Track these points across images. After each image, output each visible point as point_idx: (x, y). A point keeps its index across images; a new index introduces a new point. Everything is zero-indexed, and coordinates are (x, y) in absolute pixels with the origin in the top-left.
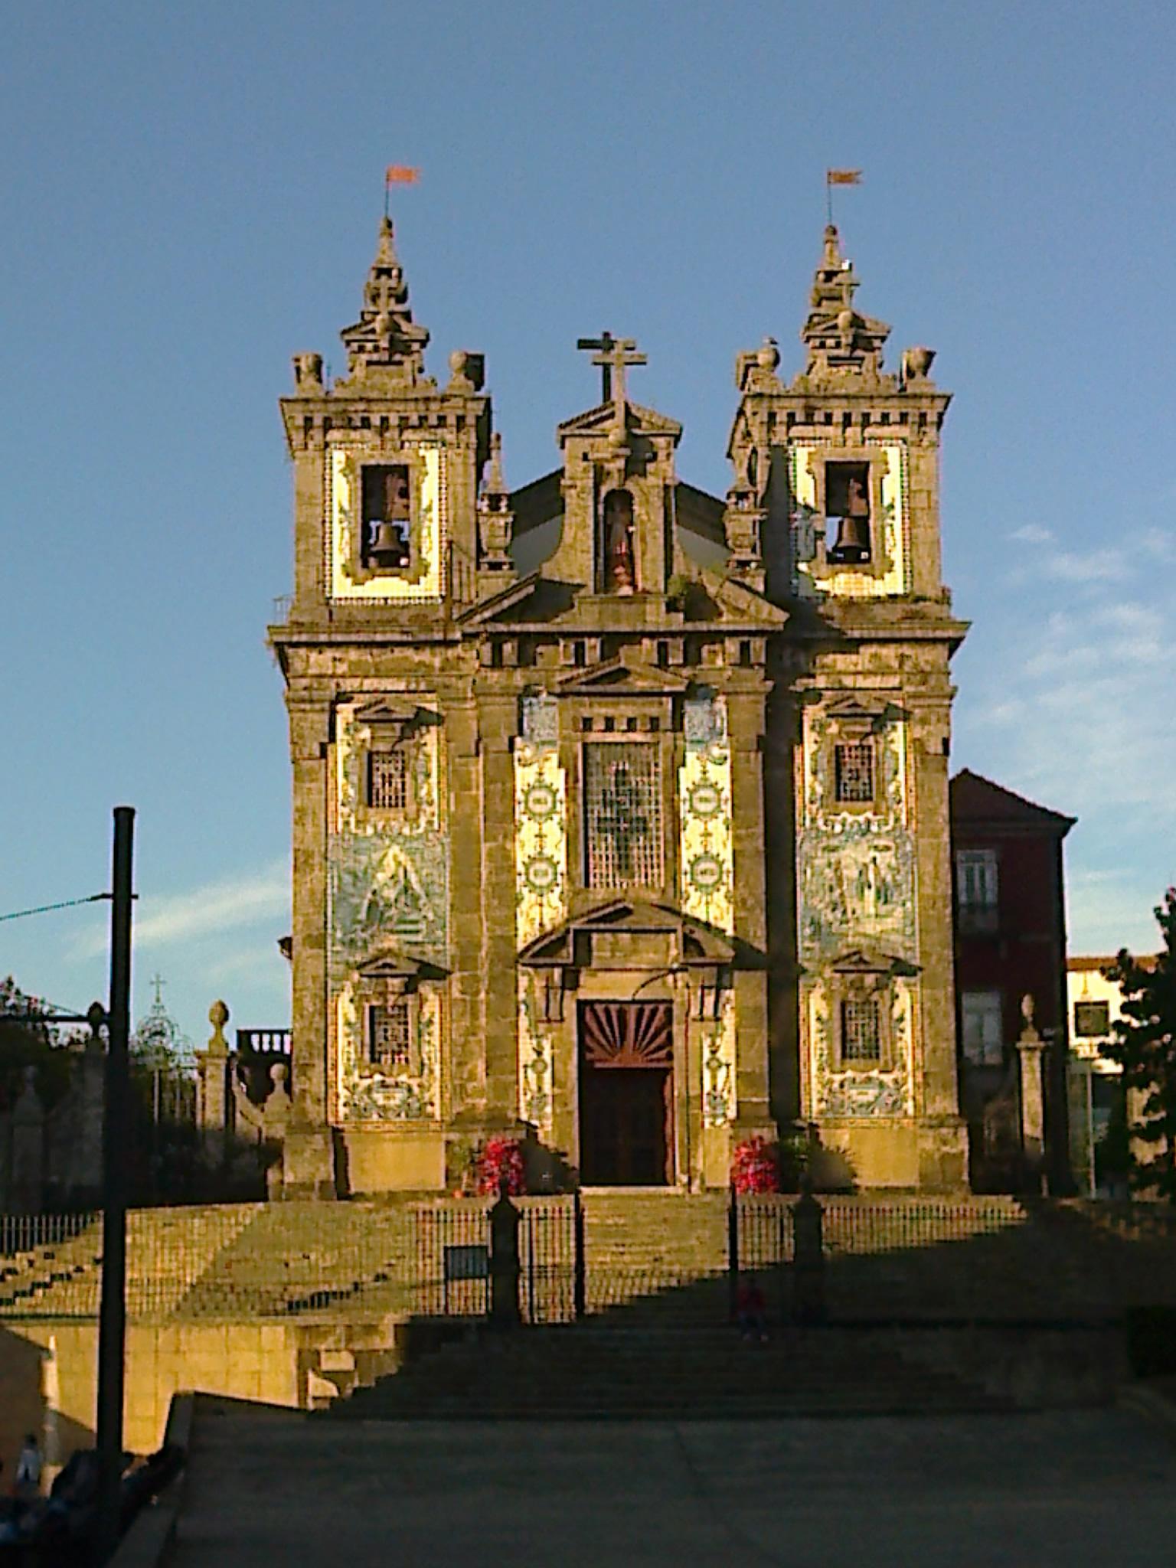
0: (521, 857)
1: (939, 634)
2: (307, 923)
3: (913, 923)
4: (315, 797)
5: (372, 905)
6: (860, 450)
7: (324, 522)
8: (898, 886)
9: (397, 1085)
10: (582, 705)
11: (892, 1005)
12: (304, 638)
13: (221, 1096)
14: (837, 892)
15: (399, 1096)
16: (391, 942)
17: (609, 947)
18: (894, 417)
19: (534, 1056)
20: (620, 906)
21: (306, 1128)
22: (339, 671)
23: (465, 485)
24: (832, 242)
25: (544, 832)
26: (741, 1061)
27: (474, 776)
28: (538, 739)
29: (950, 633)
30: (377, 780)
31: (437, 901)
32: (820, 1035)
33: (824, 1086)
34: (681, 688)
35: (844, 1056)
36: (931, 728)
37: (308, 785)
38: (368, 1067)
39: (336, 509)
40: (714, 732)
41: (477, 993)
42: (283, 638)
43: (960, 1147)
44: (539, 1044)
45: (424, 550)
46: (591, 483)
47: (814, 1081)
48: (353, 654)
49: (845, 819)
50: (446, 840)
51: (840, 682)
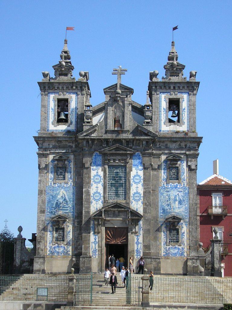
2: (41, 207)
5: (57, 203)
6: (177, 96)
8: (184, 201)
9: (61, 247)
10: (107, 155)
13: (20, 248)
16: (61, 213)
17: (112, 214)
19: (94, 240)
22: (50, 147)
24: (173, 45)
25: (98, 186)
29: (198, 140)
32: (164, 237)
35: (170, 241)
37: (42, 174)
39: (50, 108)
47: (162, 247)
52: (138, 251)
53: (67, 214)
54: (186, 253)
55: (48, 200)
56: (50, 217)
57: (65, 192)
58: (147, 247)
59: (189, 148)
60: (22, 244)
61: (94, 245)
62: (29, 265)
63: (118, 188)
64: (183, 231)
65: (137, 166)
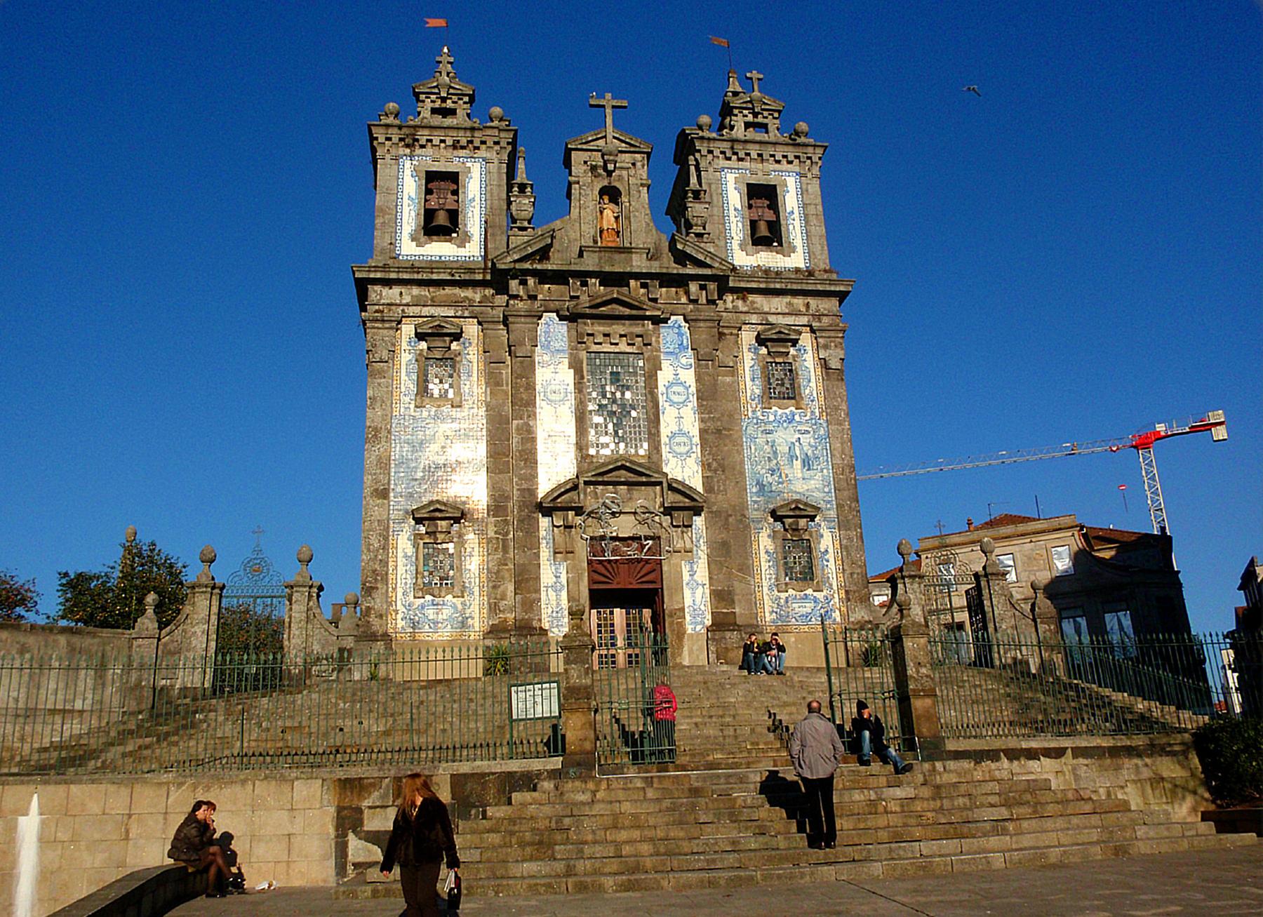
3: (829, 483)
7: (397, 205)
11: (819, 543)
12: (379, 275)
14: (775, 461)
15: (446, 612)
19: (554, 579)
20: (619, 464)
21: (373, 637)
22: (404, 302)
23: (499, 185)
26: (714, 582)
27: (504, 376)
34: (659, 313)
36: (831, 351)
37: (379, 381)
38: (421, 589)
39: (406, 197)
41: (507, 533)
45: (469, 226)
47: (766, 598)
48: (416, 291)
51: (767, 320)
54: (838, 612)
55: (397, 457)
56: (407, 512)
58: (721, 596)
60: (309, 600)
61: (554, 594)
62: (333, 671)
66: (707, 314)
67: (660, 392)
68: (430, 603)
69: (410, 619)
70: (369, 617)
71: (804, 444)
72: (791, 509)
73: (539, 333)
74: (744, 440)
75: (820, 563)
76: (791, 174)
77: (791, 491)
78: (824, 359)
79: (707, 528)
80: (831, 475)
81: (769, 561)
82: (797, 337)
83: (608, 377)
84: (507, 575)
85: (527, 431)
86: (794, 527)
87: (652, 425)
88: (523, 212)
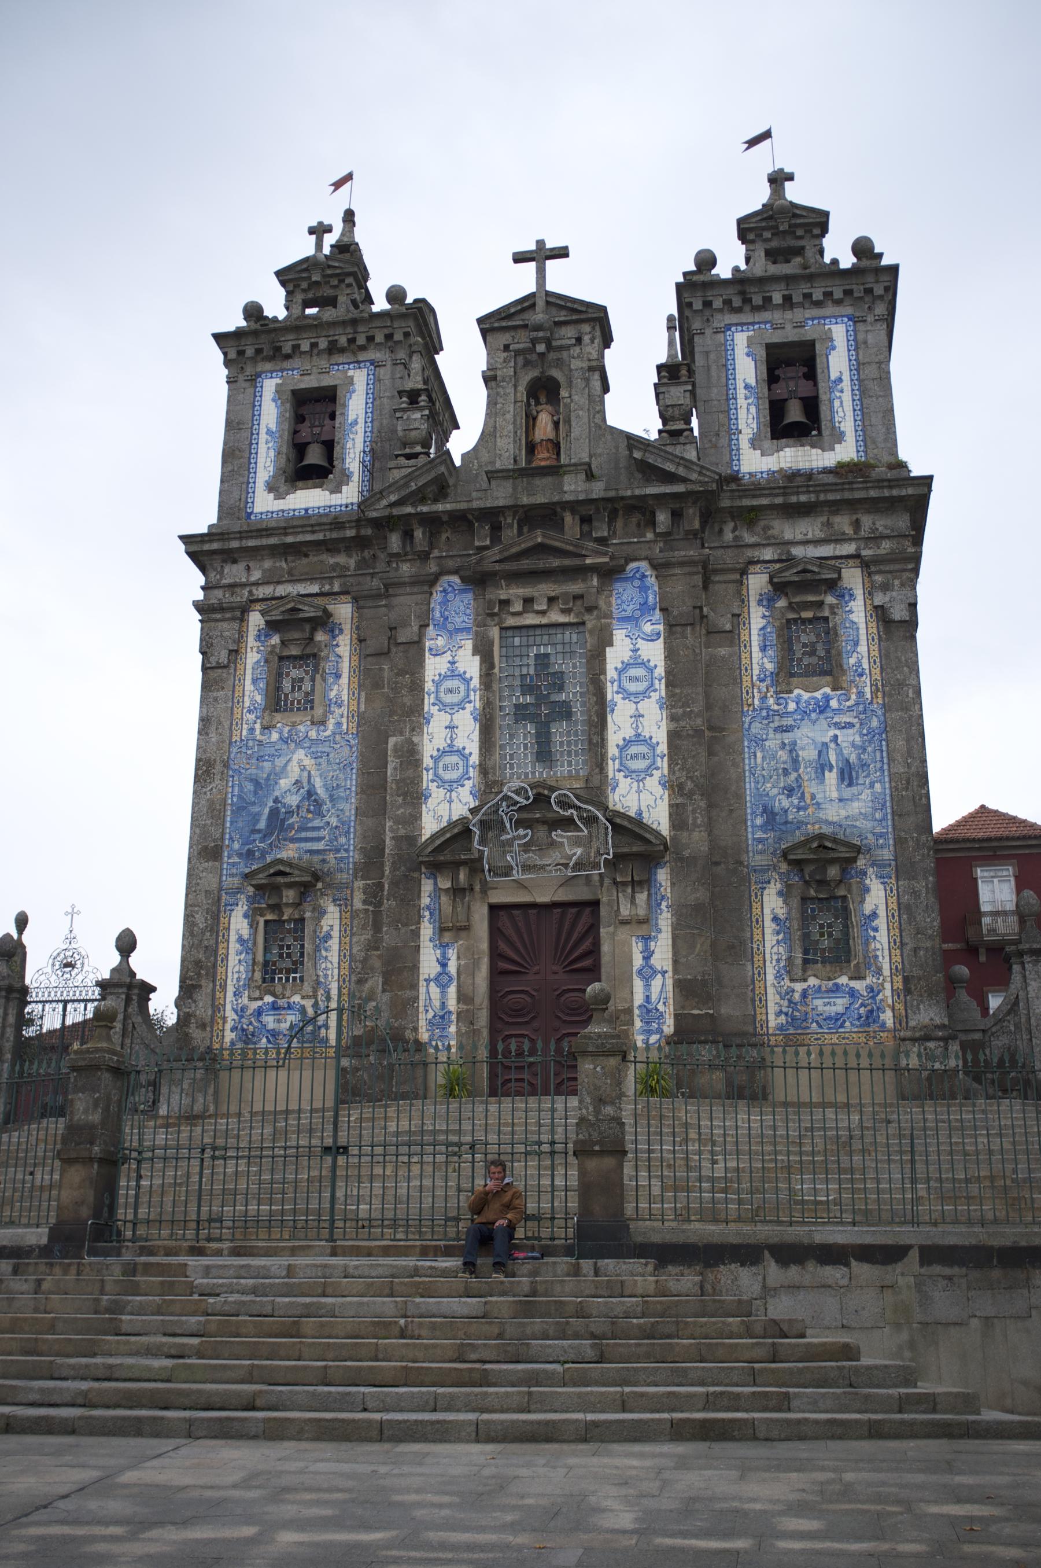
0: (429, 749)
1: (895, 492)
3: (884, 805)
4: (221, 706)
5: (274, 813)
7: (251, 444)
8: (864, 765)
9: (289, 1007)
10: (498, 586)
12: (215, 546)
14: (794, 775)
16: (289, 852)
18: (838, 294)
19: (438, 969)
22: (253, 579)
25: (456, 723)
28: (450, 627)
30: (287, 685)
31: (341, 805)
33: (782, 998)
34: (606, 559)
35: (806, 961)
36: (894, 594)
37: (215, 694)
38: (259, 987)
40: (645, 608)
41: (380, 904)
42: (194, 548)
43: (952, 1063)
44: (444, 954)
45: (347, 461)
46: (511, 372)
47: (771, 991)
48: (267, 564)
49: (799, 696)
50: (353, 742)
51: (789, 552)
52: (649, 1012)
53: (316, 858)
55: (235, 799)
57: (313, 761)
59: (874, 530)
61: (438, 990)
63: (547, 724)
64: (868, 908)
65: (637, 619)
66: (683, 553)
67: (609, 678)
68: (270, 1006)
69: (243, 1030)
70: (188, 1026)
71: (844, 745)
72: (810, 848)
73: (432, 606)
74: (746, 744)
75: (864, 933)
76: (839, 320)
77: (820, 821)
78: (882, 607)
79: (673, 884)
80: (888, 792)
81: (778, 933)
82: (835, 576)
83: (532, 662)
84: (377, 964)
85: (408, 751)
86: (818, 878)
87: (593, 729)
88: (413, 433)
